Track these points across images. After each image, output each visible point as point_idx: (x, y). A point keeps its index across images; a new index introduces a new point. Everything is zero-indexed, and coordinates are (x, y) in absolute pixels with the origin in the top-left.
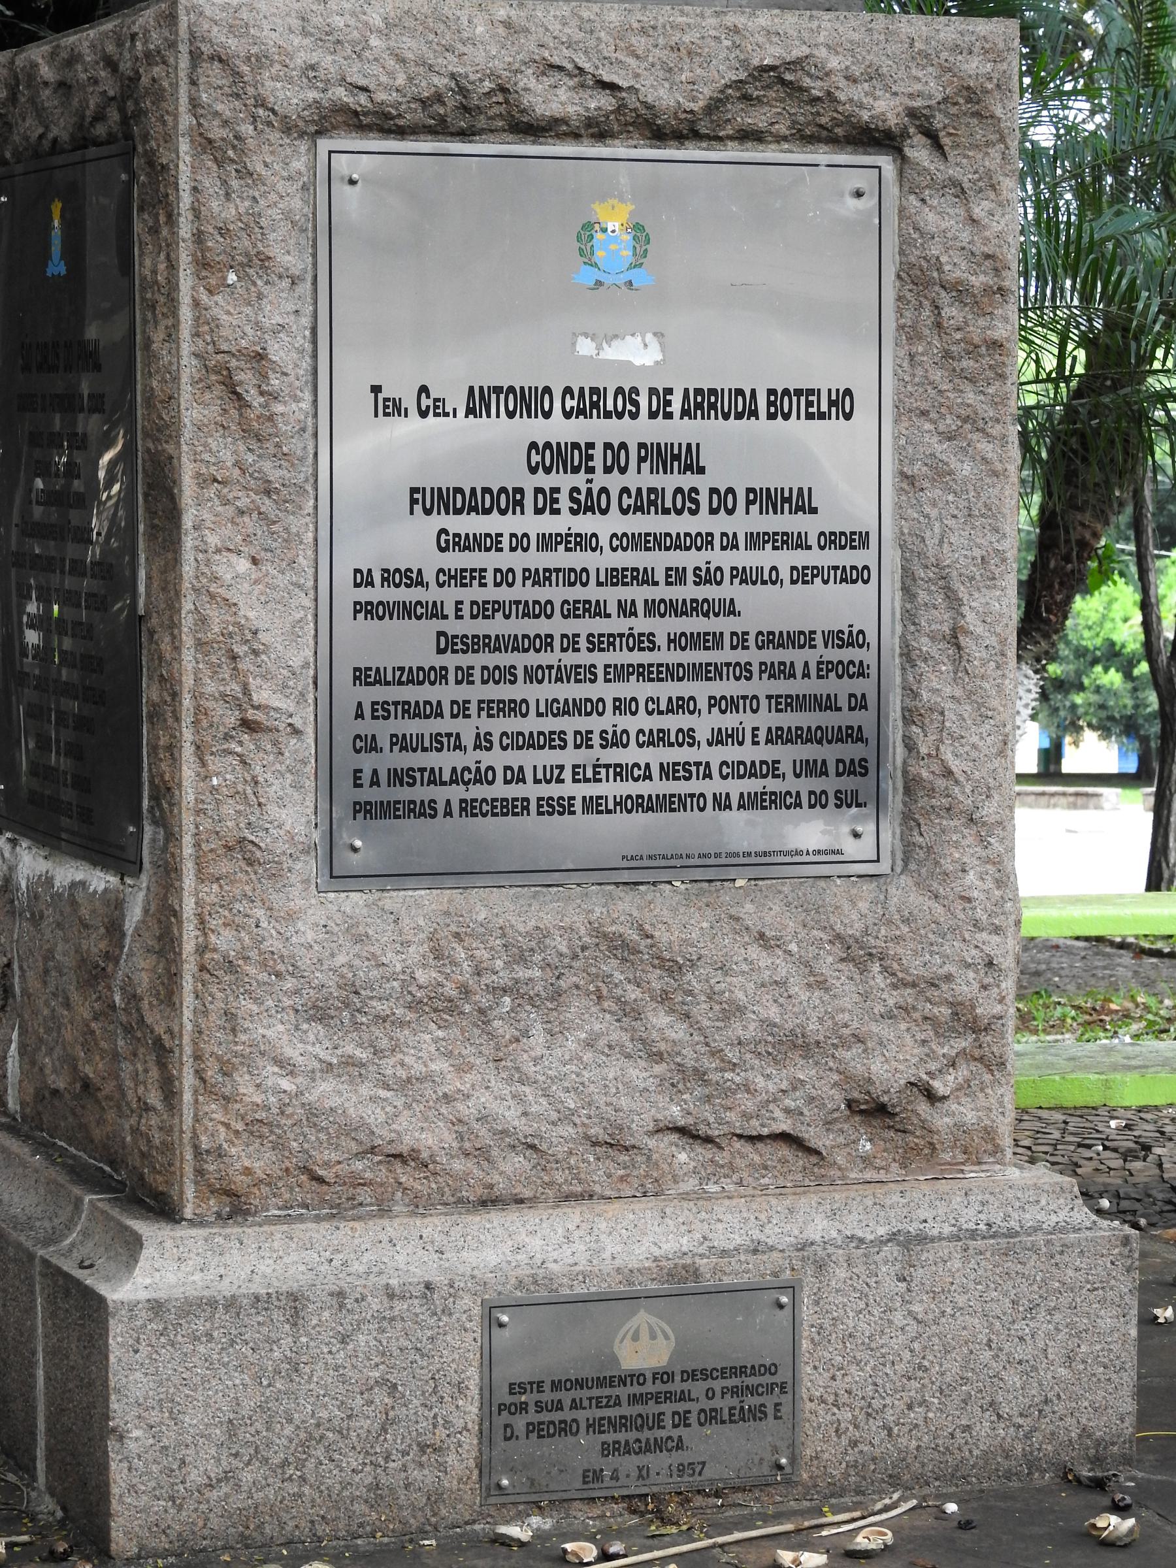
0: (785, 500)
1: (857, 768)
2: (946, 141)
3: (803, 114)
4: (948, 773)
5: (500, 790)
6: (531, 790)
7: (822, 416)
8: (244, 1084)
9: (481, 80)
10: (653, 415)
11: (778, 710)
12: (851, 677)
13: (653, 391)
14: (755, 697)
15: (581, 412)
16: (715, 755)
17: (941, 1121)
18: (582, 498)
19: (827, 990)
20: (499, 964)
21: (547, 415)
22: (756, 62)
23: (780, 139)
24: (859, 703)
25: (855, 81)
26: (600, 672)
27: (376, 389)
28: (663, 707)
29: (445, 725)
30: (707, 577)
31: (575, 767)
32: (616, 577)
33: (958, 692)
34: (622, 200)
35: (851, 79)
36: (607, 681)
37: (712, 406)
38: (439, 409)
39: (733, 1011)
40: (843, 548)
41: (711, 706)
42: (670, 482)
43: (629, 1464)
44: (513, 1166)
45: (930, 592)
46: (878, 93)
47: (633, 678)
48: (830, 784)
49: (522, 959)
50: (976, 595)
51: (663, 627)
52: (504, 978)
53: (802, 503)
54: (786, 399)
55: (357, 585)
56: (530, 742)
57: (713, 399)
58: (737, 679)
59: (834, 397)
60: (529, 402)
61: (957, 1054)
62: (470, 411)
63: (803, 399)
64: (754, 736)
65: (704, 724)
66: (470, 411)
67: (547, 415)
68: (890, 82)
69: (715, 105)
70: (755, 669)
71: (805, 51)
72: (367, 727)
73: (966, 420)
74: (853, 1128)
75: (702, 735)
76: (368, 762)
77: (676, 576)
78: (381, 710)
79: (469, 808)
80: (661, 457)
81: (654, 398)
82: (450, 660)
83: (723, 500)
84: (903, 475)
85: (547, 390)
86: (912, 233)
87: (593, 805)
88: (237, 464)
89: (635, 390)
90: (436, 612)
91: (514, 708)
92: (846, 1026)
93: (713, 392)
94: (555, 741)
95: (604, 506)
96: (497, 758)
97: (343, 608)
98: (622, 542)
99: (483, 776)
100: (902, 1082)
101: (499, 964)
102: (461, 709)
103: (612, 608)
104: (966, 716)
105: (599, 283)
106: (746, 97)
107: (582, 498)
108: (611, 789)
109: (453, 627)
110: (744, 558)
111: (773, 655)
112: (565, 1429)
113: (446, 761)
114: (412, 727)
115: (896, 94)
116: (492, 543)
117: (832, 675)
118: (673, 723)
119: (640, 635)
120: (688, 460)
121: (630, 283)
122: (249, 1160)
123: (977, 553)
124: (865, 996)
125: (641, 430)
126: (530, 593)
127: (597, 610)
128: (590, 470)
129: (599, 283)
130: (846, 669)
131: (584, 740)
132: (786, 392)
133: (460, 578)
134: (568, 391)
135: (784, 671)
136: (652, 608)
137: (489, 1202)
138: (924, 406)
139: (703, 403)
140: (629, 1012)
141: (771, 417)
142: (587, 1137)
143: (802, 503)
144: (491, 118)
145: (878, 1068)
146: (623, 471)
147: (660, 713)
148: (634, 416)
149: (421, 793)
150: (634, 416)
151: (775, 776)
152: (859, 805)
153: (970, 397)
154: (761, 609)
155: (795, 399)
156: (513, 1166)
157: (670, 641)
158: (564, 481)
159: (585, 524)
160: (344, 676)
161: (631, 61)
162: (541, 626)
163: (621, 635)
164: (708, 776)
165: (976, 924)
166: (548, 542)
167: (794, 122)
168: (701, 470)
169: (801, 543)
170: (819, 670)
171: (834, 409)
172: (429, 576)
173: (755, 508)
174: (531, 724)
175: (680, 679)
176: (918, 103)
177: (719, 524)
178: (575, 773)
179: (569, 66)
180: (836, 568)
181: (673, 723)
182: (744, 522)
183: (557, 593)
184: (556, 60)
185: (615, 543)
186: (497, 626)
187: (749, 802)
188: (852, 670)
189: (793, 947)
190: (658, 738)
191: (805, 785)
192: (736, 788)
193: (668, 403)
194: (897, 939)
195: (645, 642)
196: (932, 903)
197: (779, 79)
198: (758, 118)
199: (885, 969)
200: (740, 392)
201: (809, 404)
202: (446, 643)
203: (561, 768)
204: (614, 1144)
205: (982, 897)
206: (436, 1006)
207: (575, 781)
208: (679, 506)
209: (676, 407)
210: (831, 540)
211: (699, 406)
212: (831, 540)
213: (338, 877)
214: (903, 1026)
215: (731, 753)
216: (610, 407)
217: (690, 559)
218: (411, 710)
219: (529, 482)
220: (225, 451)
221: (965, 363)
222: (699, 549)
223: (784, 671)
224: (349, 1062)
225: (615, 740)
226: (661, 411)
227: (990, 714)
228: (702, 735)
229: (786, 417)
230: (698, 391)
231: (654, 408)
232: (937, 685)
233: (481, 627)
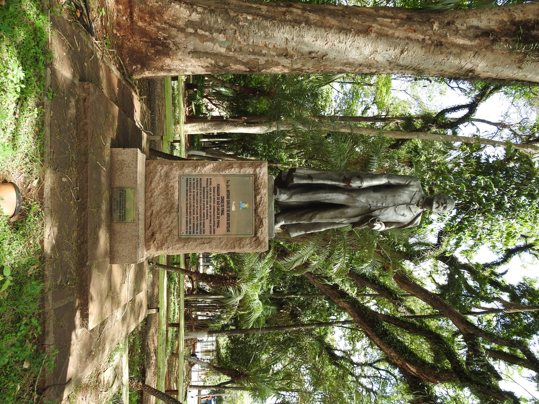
1: (190, 233)
3: (258, 225)
5: (189, 193)
6: (189, 197)
8: (160, 166)
16: (192, 217)
17: (151, 242)
29: (196, 188)
32: (210, 206)
38: (227, 187)
39: (164, 218)
42: (220, 212)
43: (116, 203)
44: (149, 195)
48: (189, 230)
49: (171, 195)
51: (205, 211)
53: (218, 226)
56: (194, 197)
60: (228, 197)
65: (195, 216)
69: (258, 215)
72: (196, 180)
74: (151, 233)
76: (192, 180)
78: (197, 181)
79: (187, 190)
80: (223, 211)
83: (218, 218)
86: (246, 238)
87: (187, 204)
90: (207, 187)
91: (197, 195)
94: (194, 199)
96: (192, 193)
98: (214, 207)
99: (190, 192)
102: (197, 189)
109: (206, 189)
111: (202, 223)
112: (120, 196)
113: (192, 188)
116: (214, 193)
118: (195, 212)
120: (222, 214)
122: (151, 167)
125: (226, 209)
126: (209, 197)
127: (207, 204)
131: (194, 202)
133: (211, 189)
135: (201, 225)
137: (146, 192)
139: (228, 215)
140: (165, 207)
149: (189, 185)
154: (207, 222)
156: (149, 194)
158: (220, 200)
159: (216, 203)
160: (201, 177)
162: (206, 198)
166: (214, 199)
169: (214, 226)
177: (216, 217)
181: (195, 212)
182: (216, 220)
183: (209, 200)
186: (206, 193)
190: (194, 211)
191: (188, 227)
192: (188, 219)
195: (204, 209)
197: (261, 222)
198: (257, 220)
202: (204, 188)
204: (151, 206)
206: (167, 186)
212: (214, 230)
213: (180, 177)
215: (192, 219)
217: (212, 214)
220: (223, 165)
223: (201, 225)
225: (194, 206)
232: (199, 241)
233: (206, 192)
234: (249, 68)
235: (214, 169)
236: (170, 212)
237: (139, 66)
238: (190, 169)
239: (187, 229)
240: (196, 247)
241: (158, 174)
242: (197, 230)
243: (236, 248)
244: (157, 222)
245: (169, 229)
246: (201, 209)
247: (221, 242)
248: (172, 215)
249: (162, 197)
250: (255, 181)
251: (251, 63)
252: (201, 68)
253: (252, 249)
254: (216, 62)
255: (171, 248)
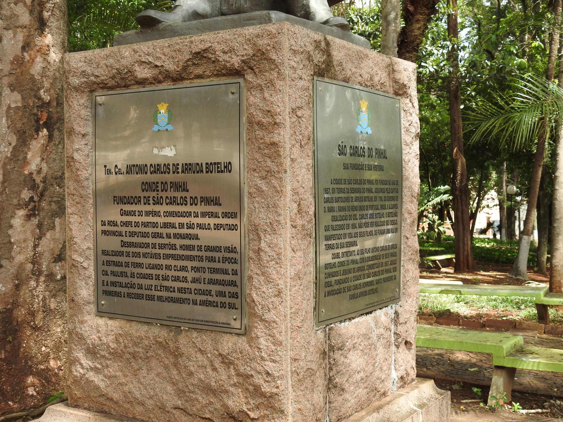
0: (212, 201)
2: (257, 70)
3: (211, 66)
4: (254, 301)
5: (136, 291)
7: (222, 172)
9: (124, 69)
11: (211, 273)
12: (232, 263)
14: (204, 268)
18: (156, 199)
19: (217, 372)
20: (130, 345)
22: (193, 52)
23: (209, 77)
24: (235, 273)
25: (227, 53)
26: (162, 256)
27: (105, 166)
28: (179, 269)
30: (190, 226)
31: (155, 286)
33: (259, 272)
34: (165, 103)
35: (225, 52)
36: (164, 259)
37: (190, 169)
39: (191, 374)
40: (229, 218)
41: (192, 270)
42: (179, 194)
45: (253, 235)
46: (233, 56)
47: (170, 258)
48: (227, 300)
49: (136, 344)
50: (268, 236)
51: (179, 242)
52: (131, 350)
55: (102, 225)
58: (199, 261)
61: (259, 404)
62: (127, 173)
64: (204, 281)
65: (190, 275)
68: (236, 52)
69: (185, 68)
70: (204, 258)
71: (210, 45)
73: (268, 172)
75: (189, 279)
76: (105, 278)
77: (181, 226)
78: (109, 263)
79: (129, 295)
82: (125, 249)
84: (250, 193)
85: (146, 165)
88: (74, 189)
89: (169, 164)
91: (140, 265)
92: (223, 386)
93: (190, 164)
94: (149, 277)
96: (136, 281)
97: (99, 233)
100: (238, 410)
101: (130, 345)
103: (165, 236)
104: (261, 281)
105: (159, 130)
106: (194, 64)
107: (156, 199)
108: (164, 294)
109: (126, 239)
110: (200, 220)
114: (116, 269)
115: (238, 56)
117: (227, 262)
118: (182, 274)
119: (173, 244)
121: (167, 130)
123: (268, 221)
124: (229, 377)
125: (170, 177)
127: (160, 236)
128: (158, 191)
129: (159, 130)
130: (231, 260)
133: (126, 224)
134: (151, 165)
135: (211, 259)
136: (176, 236)
138: (255, 167)
140: (166, 367)
141: (207, 172)
142: (157, 405)
143: (216, 202)
144: (130, 81)
145: (230, 403)
146: (166, 191)
147: (178, 271)
149: (118, 289)
151: (210, 295)
152: (236, 309)
153: (269, 163)
157: (180, 247)
159: (157, 208)
161: (163, 57)
163: (167, 244)
164: (191, 293)
165: (262, 358)
167: (211, 70)
168: (188, 191)
170: (223, 260)
172: (119, 223)
173: (203, 203)
174: (144, 271)
175: (183, 260)
176: (245, 58)
178: (155, 288)
179: (147, 61)
180: (227, 225)
181: (182, 274)
182: (200, 208)
183: (150, 230)
184: (144, 60)
185: (165, 214)
187: (204, 303)
188: (233, 261)
189: (209, 355)
190: (177, 279)
191: (219, 299)
193: (178, 168)
194: (238, 359)
195: (173, 247)
196: (248, 348)
197: (200, 56)
199: (234, 368)
200: (198, 164)
201: (218, 168)
202: (124, 244)
203: (152, 285)
205: (265, 348)
206: (116, 355)
207: (155, 290)
210: (226, 215)
211: (186, 169)
213: (100, 313)
214: (240, 390)
217: (185, 220)
218: (116, 264)
219: (142, 194)
221: (266, 151)
222: (188, 217)
223: (211, 259)
224: (96, 367)
225: (166, 278)
226: (176, 172)
227: (272, 281)
228: (189, 279)
230: (186, 164)
234: (37, 130)
235: (83, 214)
236: (177, 354)
237: (30, 380)
238: (81, 283)
239: (223, 305)
240: (268, 280)
241: (91, 376)
242: (225, 272)
243: (276, 139)
244: (203, 399)
245: (217, 364)
246: (173, 257)
247: (260, 190)
248: (183, 349)
249: (144, 372)
250: (104, 86)
251: (19, 125)
252: (44, 241)
253: (279, 84)
254: (19, 206)
255: (269, 366)
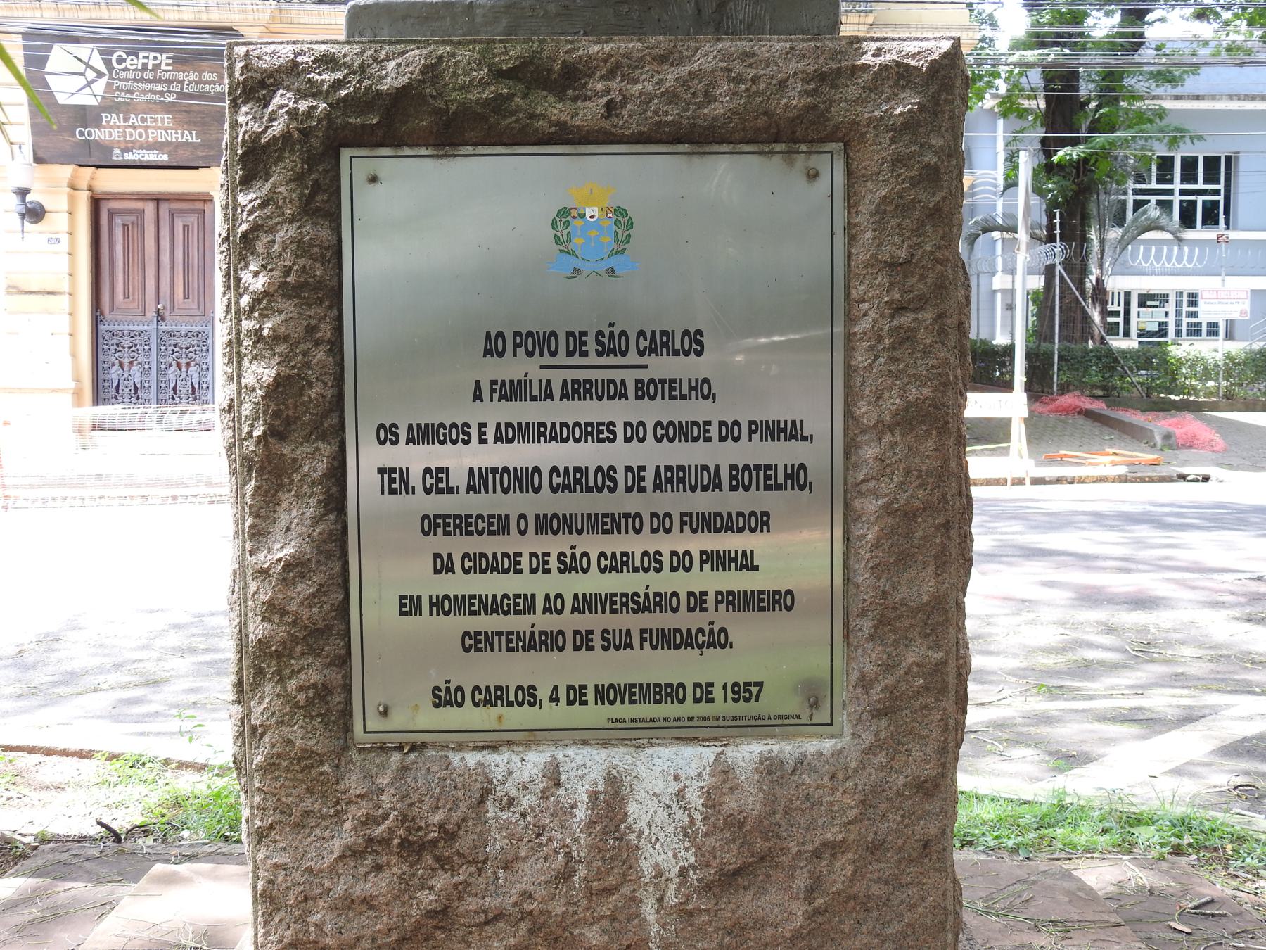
7: (778, 487)
10: (629, 489)
13: (628, 469)
15: (566, 487)
21: (537, 490)
37: (681, 480)
54: (746, 473)
57: (681, 474)
59: (789, 471)
62: (471, 488)
63: (761, 473)
66: (471, 488)
67: (537, 490)
81: (630, 474)
95: (585, 566)
132: (746, 467)
141: (733, 488)
148: (612, 490)
150: (612, 490)
155: (754, 473)
171: (789, 482)
193: (642, 479)
200: (705, 468)
201: (767, 477)
208: (646, 565)
209: (649, 482)
211: (669, 481)
216: (591, 483)
229: (747, 488)
230: (668, 468)
231: (630, 484)
